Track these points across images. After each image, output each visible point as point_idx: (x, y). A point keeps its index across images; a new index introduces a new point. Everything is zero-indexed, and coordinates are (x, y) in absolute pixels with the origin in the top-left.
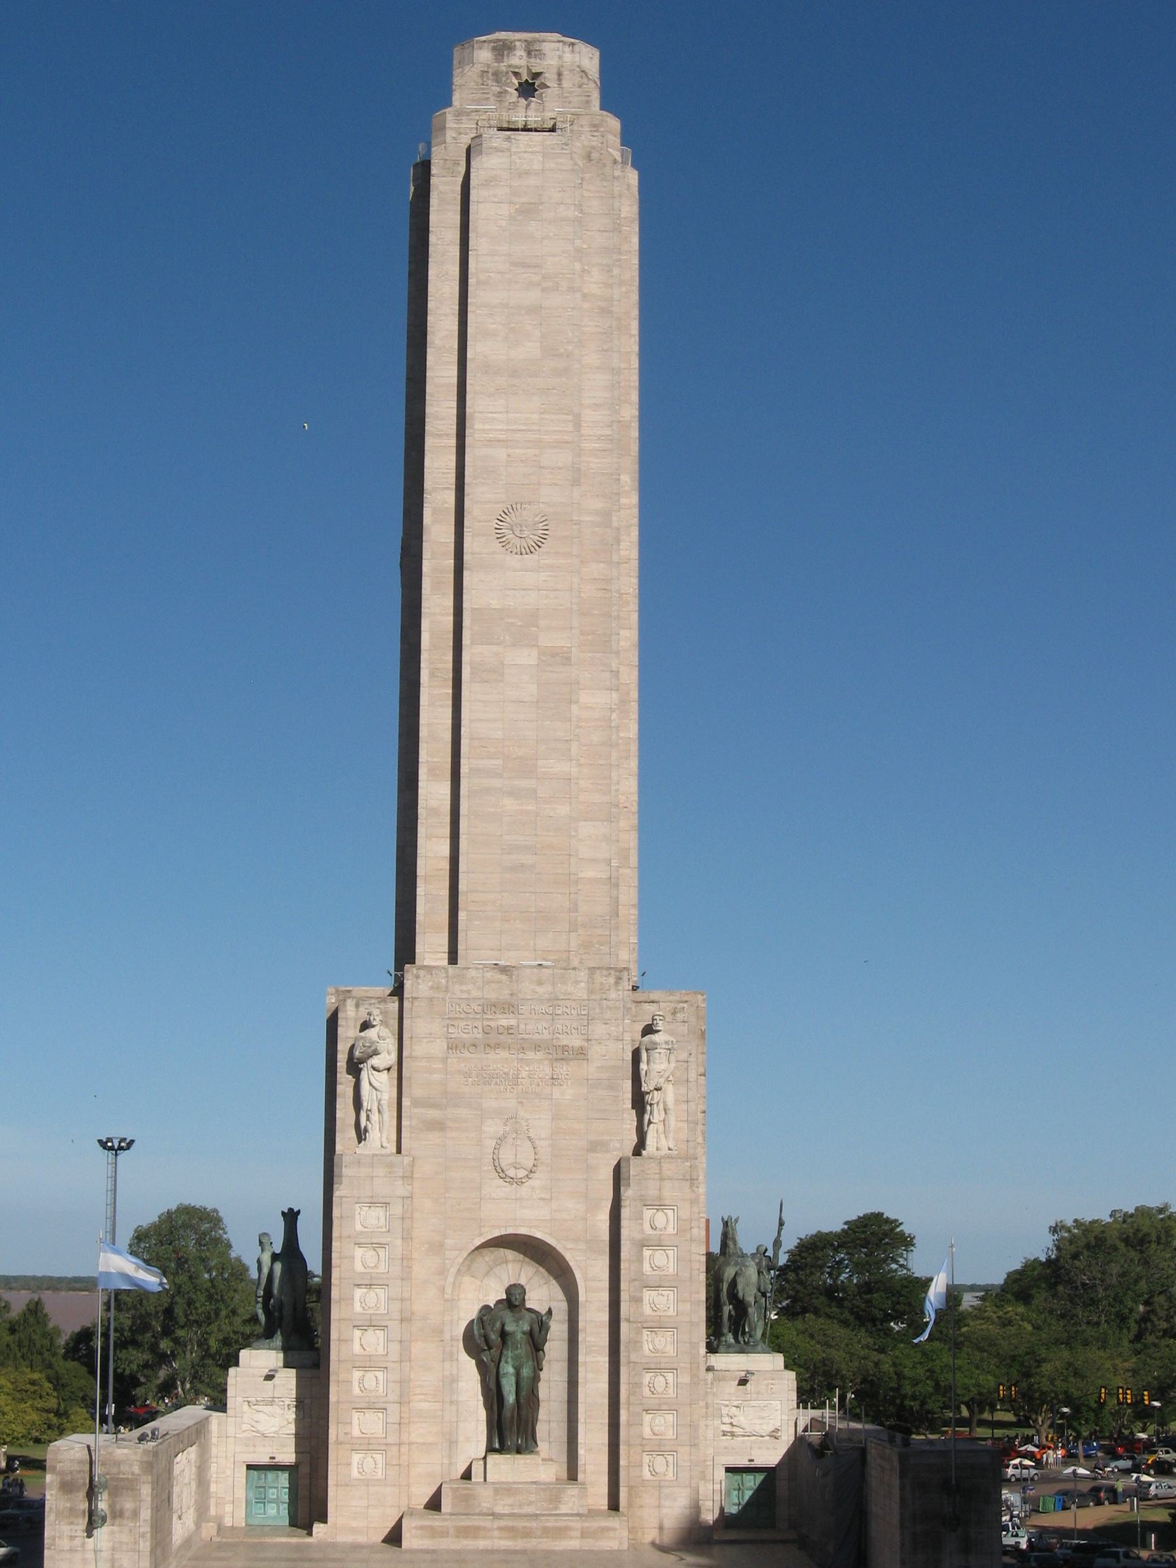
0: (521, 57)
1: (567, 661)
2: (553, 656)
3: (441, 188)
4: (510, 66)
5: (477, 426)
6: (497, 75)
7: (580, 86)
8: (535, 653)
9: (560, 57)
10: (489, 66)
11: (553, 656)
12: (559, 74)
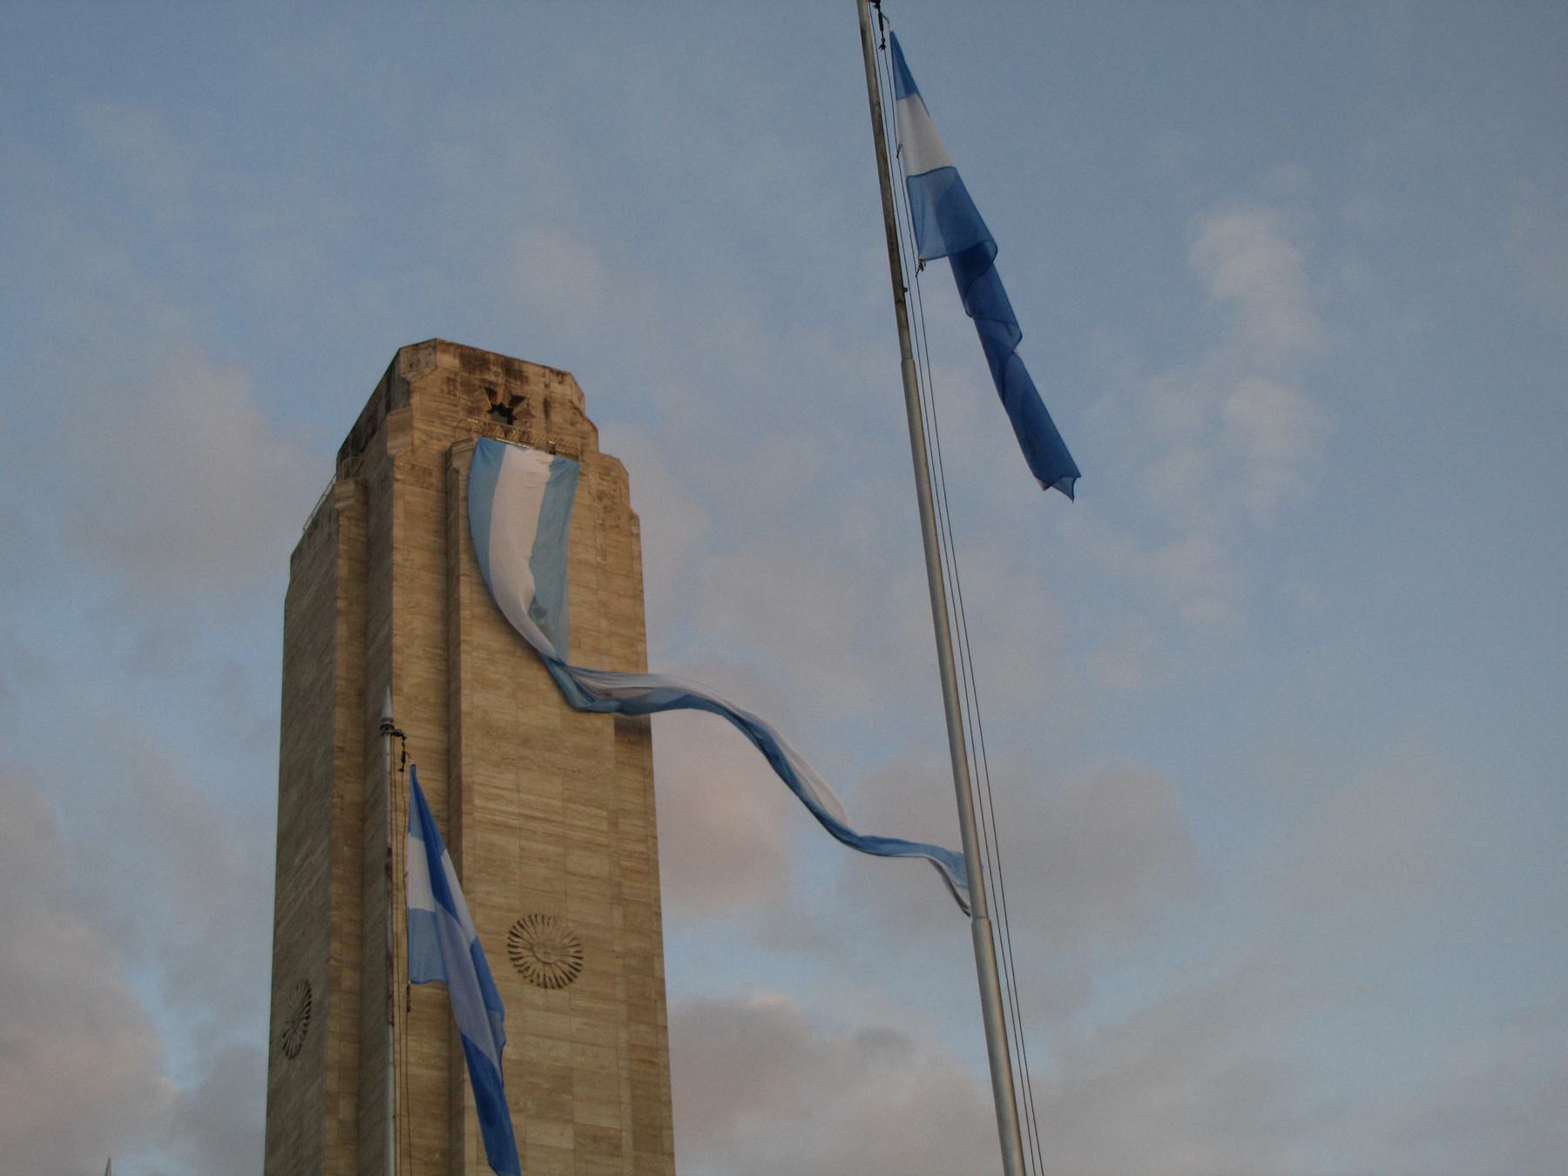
0: (497, 375)
1: (615, 1149)
2: (595, 1139)
3: (408, 498)
4: (484, 381)
5: (478, 802)
6: (468, 387)
7: (573, 424)
8: (569, 1132)
9: (547, 386)
10: (456, 374)
11: (595, 1139)
12: (547, 405)
